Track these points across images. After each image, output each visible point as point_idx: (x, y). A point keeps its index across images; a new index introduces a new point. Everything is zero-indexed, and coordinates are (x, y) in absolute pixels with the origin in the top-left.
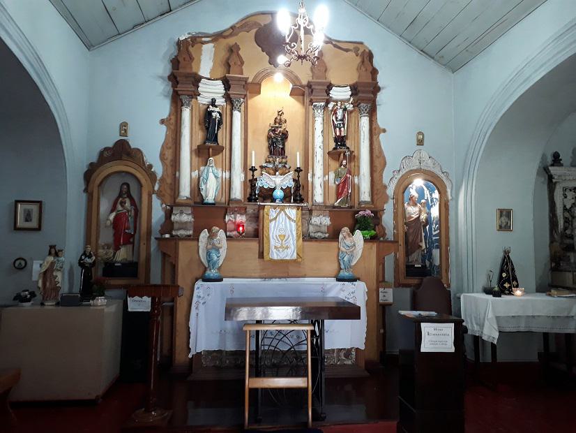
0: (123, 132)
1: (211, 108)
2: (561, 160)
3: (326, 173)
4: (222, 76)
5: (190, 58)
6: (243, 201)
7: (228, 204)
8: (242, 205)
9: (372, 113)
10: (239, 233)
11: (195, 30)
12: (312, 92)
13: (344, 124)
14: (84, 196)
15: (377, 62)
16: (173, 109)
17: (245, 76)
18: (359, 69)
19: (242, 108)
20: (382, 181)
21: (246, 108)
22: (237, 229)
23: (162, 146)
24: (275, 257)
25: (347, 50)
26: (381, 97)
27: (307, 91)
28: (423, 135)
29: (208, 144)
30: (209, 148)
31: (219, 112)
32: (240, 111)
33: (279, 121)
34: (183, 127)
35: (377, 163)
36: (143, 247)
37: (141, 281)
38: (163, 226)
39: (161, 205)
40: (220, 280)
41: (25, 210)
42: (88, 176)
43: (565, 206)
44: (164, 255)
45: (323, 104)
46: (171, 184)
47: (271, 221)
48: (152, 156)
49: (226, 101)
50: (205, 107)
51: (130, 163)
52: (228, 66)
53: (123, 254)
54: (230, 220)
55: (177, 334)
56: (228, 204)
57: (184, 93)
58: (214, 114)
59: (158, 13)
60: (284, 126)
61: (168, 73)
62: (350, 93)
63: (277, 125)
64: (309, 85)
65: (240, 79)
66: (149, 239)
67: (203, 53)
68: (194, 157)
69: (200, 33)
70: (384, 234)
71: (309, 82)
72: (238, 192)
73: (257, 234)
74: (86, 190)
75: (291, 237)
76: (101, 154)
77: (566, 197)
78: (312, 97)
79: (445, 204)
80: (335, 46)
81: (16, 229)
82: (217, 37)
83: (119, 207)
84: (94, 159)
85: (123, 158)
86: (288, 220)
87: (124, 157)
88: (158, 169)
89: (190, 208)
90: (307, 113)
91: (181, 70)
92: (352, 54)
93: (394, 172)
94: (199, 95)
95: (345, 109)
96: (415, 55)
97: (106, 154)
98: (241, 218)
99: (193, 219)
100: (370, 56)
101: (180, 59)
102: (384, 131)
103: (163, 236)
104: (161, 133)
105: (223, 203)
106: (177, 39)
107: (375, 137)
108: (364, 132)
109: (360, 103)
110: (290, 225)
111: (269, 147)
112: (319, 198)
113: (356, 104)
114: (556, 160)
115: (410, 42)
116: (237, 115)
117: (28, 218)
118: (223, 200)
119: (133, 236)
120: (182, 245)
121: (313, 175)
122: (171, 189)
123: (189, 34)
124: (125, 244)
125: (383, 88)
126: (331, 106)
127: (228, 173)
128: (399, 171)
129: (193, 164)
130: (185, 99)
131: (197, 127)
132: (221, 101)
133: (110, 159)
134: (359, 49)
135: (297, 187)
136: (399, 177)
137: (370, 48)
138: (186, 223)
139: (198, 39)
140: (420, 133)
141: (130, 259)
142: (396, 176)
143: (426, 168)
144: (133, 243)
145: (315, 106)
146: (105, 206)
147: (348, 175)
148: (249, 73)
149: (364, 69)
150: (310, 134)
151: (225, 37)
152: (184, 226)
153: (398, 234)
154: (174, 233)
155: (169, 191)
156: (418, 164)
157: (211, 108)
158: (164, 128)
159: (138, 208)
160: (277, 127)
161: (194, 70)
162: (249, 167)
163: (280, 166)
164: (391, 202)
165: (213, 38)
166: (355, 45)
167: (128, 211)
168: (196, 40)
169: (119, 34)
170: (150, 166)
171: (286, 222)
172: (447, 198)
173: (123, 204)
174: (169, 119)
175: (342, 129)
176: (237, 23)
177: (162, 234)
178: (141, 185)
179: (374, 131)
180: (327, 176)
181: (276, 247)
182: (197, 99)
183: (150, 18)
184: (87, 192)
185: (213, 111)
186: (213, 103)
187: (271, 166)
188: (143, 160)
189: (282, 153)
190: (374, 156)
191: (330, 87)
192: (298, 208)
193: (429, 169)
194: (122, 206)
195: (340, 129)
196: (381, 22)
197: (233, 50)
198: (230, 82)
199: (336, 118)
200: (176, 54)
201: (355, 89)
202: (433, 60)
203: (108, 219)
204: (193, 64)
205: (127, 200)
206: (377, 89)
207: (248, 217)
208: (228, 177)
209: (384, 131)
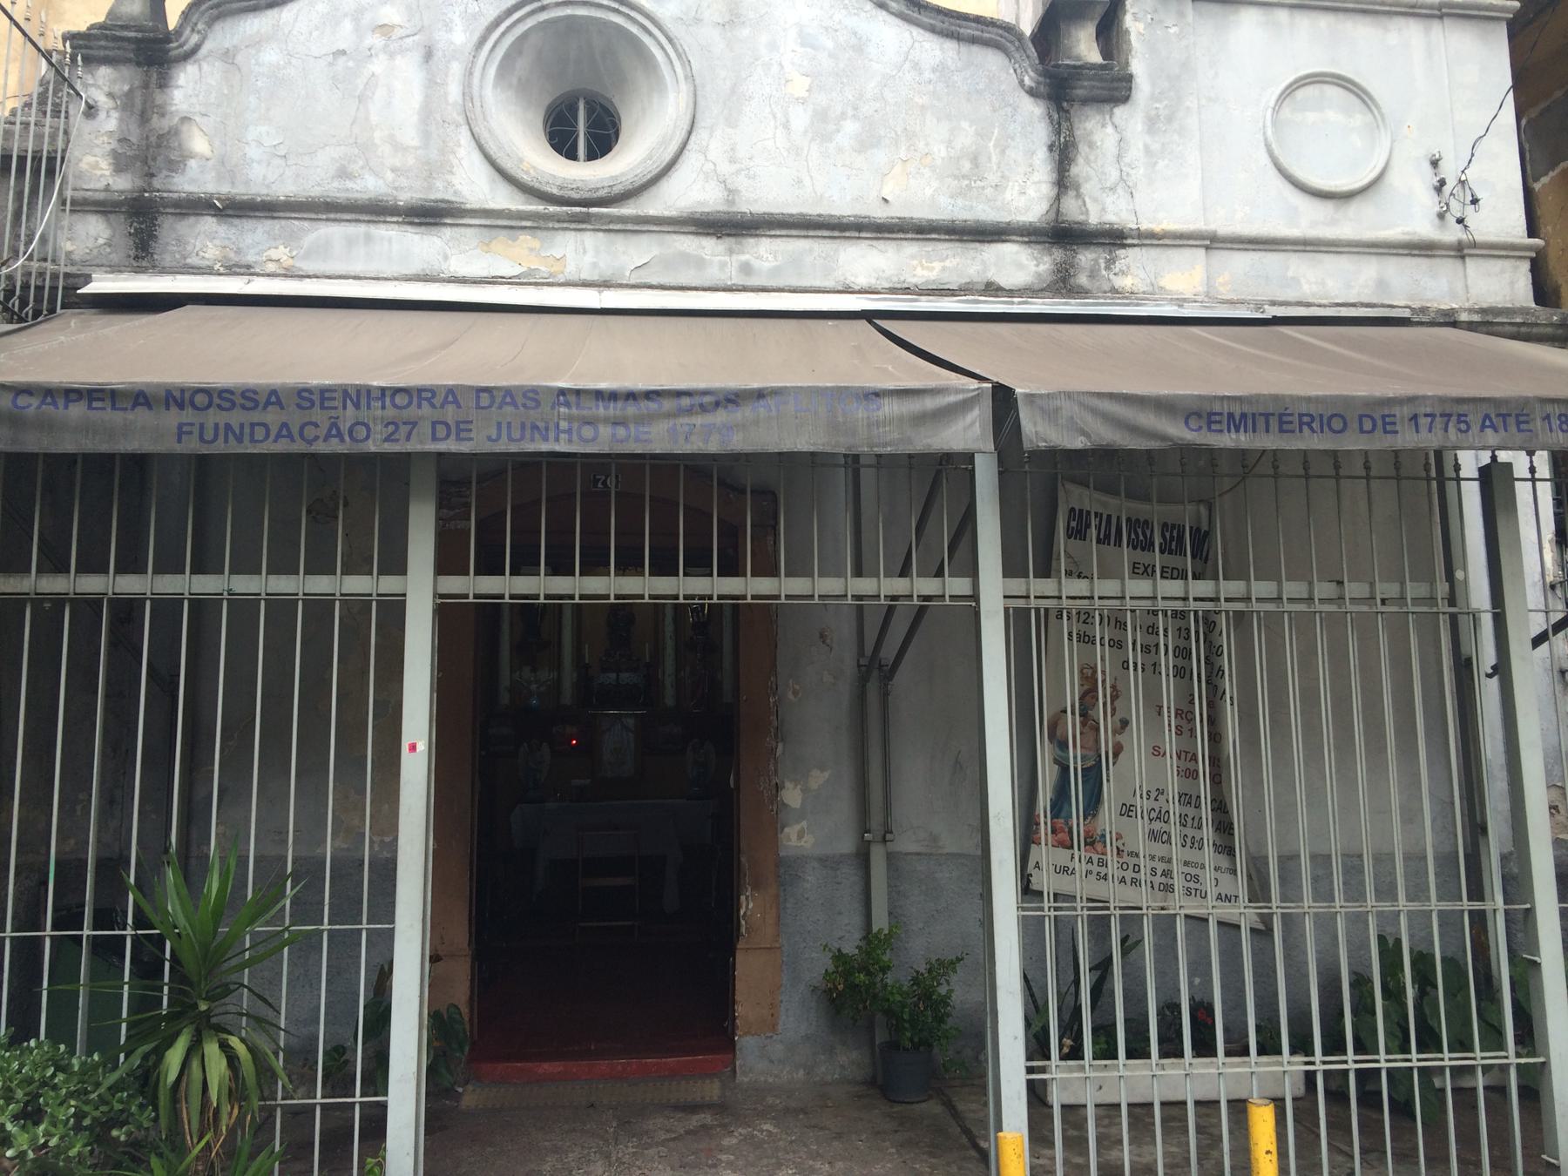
112: (670, 701)
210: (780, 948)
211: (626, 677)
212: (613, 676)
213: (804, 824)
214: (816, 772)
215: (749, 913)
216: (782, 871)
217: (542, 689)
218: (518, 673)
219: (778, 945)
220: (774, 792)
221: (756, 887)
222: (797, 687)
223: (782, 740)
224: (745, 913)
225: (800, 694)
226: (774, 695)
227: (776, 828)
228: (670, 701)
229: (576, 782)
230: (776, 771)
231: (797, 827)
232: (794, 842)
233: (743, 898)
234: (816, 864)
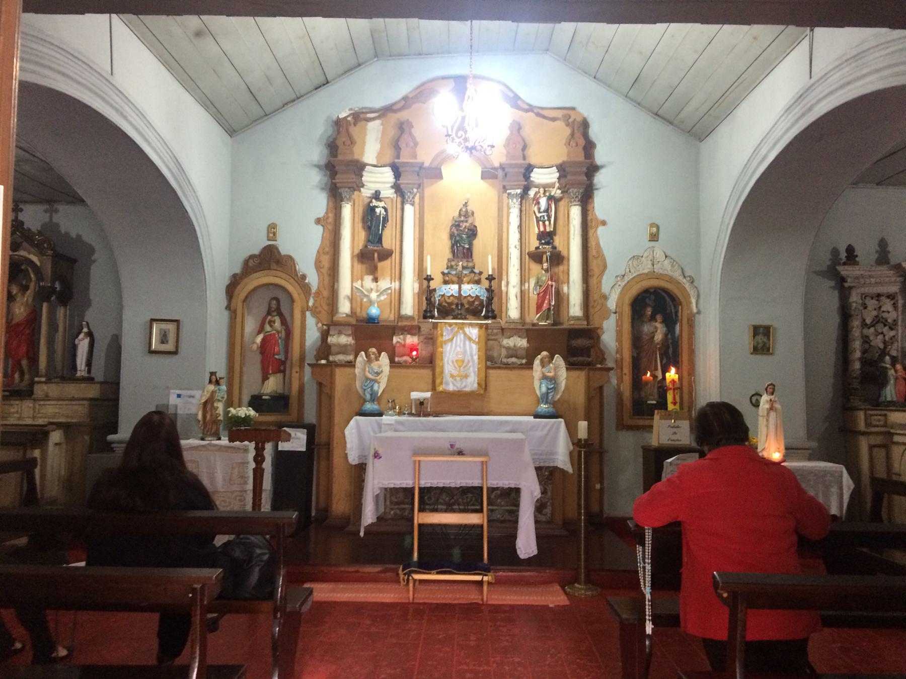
0: (271, 235)
1: (375, 203)
2: (857, 256)
3: (523, 281)
4: (392, 161)
5: (352, 143)
6: (416, 318)
7: (398, 323)
8: (416, 323)
9: (586, 199)
10: (412, 358)
11: (357, 105)
12: (506, 175)
14: (226, 314)
15: (595, 132)
16: (331, 204)
17: (420, 159)
18: (568, 144)
19: (417, 199)
20: (600, 289)
21: (422, 199)
22: (410, 355)
23: (318, 252)
24: (451, 388)
25: (554, 119)
26: (600, 178)
27: (500, 173)
28: (658, 227)
29: (370, 247)
30: (373, 252)
31: (384, 208)
32: (413, 205)
33: (465, 213)
34: (342, 227)
35: (594, 265)
36: (295, 376)
37: (293, 416)
38: (319, 350)
39: (317, 325)
40: (381, 415)
41: (161, 330)
42: (231, 290)
43: (864, 320)
44: (320, 385)
45: (519, 191)
46: (328, 298)
47: (446, 342)
48: (307, 266)
49: (396, 192)
50: (369, 200)
51: (280, 274)
52: (397, 147)
53: (272, 385)
54: (398, 342)
55: (334, 479)
56: (398, 323)
57: (344, 185)
58: (378, 210)
59: (312, 87)
60: (470, 220)
61: (323, 162)
62: (557, 175)
63: (462, 218)
64: (502, 167)
65: (412, 165)
66: (301, 366)
67: (368, 133)
68: (356, 264)
69: (363, 108)
70: (603, 360)
71: (501, 165)
72: (409, 307)
73: (431, 362)
74: (228, 308)
75: (471, 364)
76: (246, 262)
77: (865, 308)
78: (505, 184)
79: (688, 320)
80: (538, 115)
81: (152, 352)
82: (385, 112)
83: (268, 328)
84: (237, 270)
85: (272, 268)
86: (467, 342)
87: (274, 266)
88: (313, 279)
89: (350, 327)
90: (500, 202)
91: (340, 157)
92: (560, 124)
93: (617, 277)
94: (363, 186)
95: (551, 198)
96: (647, 120)
97: (251, 263)
98: (411, 340)
99: (353, 342)
100: (585, 125)
101: (339, 143)
102: (604, 223)
103: (319, 362)
104: (316, 236)
105: (392, 321)
106: (335, 118)
107: (591, 232)
108: (574, 226)
109: (569, 189)
110: (471, 348)
111: (452, 247)
112: (513, 312)
113: (564, 189)
114: (851, 256)
115: (639, 104)
116: (409, 210)
117: (164, 339)
118: (392, 317)
119: (283, 363)
120: (339, 372)
121: (508, 283)
122: (328, 305)
123: (350, 109)
124: (274, 373)
125: (602, 167)
126: (532, 193)
127: (397, 283)
128: (624, 276)
129: (355, 273)
130: (344, 192)
131: (359, 225)
132: (388, 192)
133: (255, 270)
134: (570, 117)
135: (490, 299)
136: (624, 283)
137: (585, 115)
138: (346, 346)
139: (362, 116)
140: (652, 225)
141: (280, 390)
142: (619, 283)
143: (661, 272)
144: (284, 372)
145: (509, 194)
146: (250, 325)
147: (550, 283)
148: (425, 157)
149: (574, 144)
150: (505, 229)
151: (396, 111)
152: (343, 349)
153: (622, 359)
154: (331, 358)
155: (326, 307)
156: (650, 266)
157: (375, 203)
158: (320, 228)
159: (290, 325)
160: (463, 221)
161: (356, 157)
162: (425, 276)
163: (465, 272)
164: (613, 318)
165: (380, 113)
166: (565, 112)
167: (278, 332)
168: (359, 117)
169: (266, 115)
170: (304, 277)
171: (464, 344)
172: (691, 311)
173: (271, 323)
174: (326, 217)
175: (547, 223)
176: (411, 92)
177: (317, 360)
178: (292, 300)
179: (589, 224)
180: (527, 285)
181: (452, 376)
182: (360, 191)
183: (302, 94)
184: (230, 309)
185: (377, 207)
186: (377, 196)
187: (454, 272)
188: (295, 270)
189: (468, 254)
190: (590, 257)
191: (529, 169)
192: (481, 326)
193: (666, 272)
194: (271, 326)
195: (544, 222)
196: (598, 79)
197: (403, 128)
198: (401, 169)
199: (539, 209)
200: (334, 137)
201: (562, 169)
202: (671, 127)
203: (254, 343)
204: (356, 149)
205: (277, 320)
206: (592, 169)
207: (422, 338)
208: (397, 287)
209: (604, 223)
211: (469, 290)
212: (455, 287)
217: (382, 298)
218: (359, 282)
228: (513, 312)
229: (415, 395)
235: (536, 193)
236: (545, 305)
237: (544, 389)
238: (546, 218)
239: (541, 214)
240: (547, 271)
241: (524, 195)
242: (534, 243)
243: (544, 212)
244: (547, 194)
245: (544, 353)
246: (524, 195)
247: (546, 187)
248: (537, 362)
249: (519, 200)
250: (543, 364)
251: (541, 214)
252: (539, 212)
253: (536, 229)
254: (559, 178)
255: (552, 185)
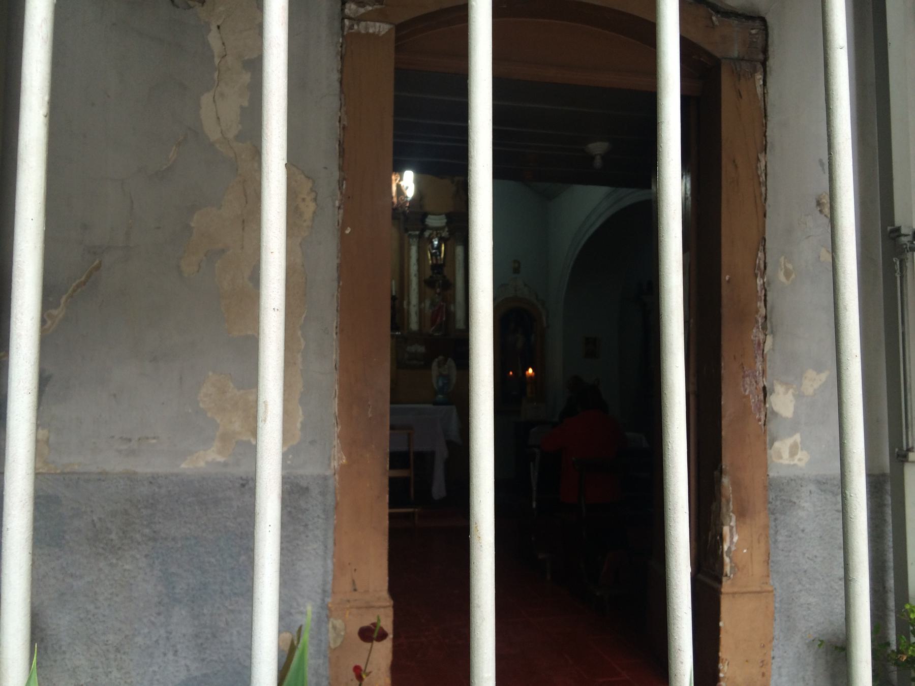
3: (421, 299)
13: (440, 252)
45: (417, 233)
62: (445, 221)
95: (441, 240)
112: (414, 325)
113: (451, 233)
147: (442, 304)
175: (439, 257)
180: (423, 305)
191: (425, 215)
201: (449, 216)
210: (772, 591)
213: (797, 437)
214: (811, 373)
215: (733, 548)
216: (772, 495)
219: (770, 589)
220: (762, 397)
221: (742, 514)
222: (790, 266)
223: (772, 332)
224: (729, 548)
225: (793, 276)
226: (763, 277)
227: (765, 443)
228: (414, 325)
230: (764, 372)
231: (789, 441)
232: (786, 459)
233: (726, 529)
234: (812, 487)
235: (430, 235)
236: (438, 320)
237: (440, 384)
238: (438, 253)
239: (434, 251)
240: (439, 294)
241: (421, 236)
242: (428, 273)
243: (436, 249)
244: (439, 235)
245: (441, 357)
246: (421, 236)
247: (436, 229)
248: (435, 364)
249: (418, 239)
250: (439, 366)
251: (434, 251)
252: (433, 249)
253: (430, 262)
254: (447, 223)
255: (442, 228)
